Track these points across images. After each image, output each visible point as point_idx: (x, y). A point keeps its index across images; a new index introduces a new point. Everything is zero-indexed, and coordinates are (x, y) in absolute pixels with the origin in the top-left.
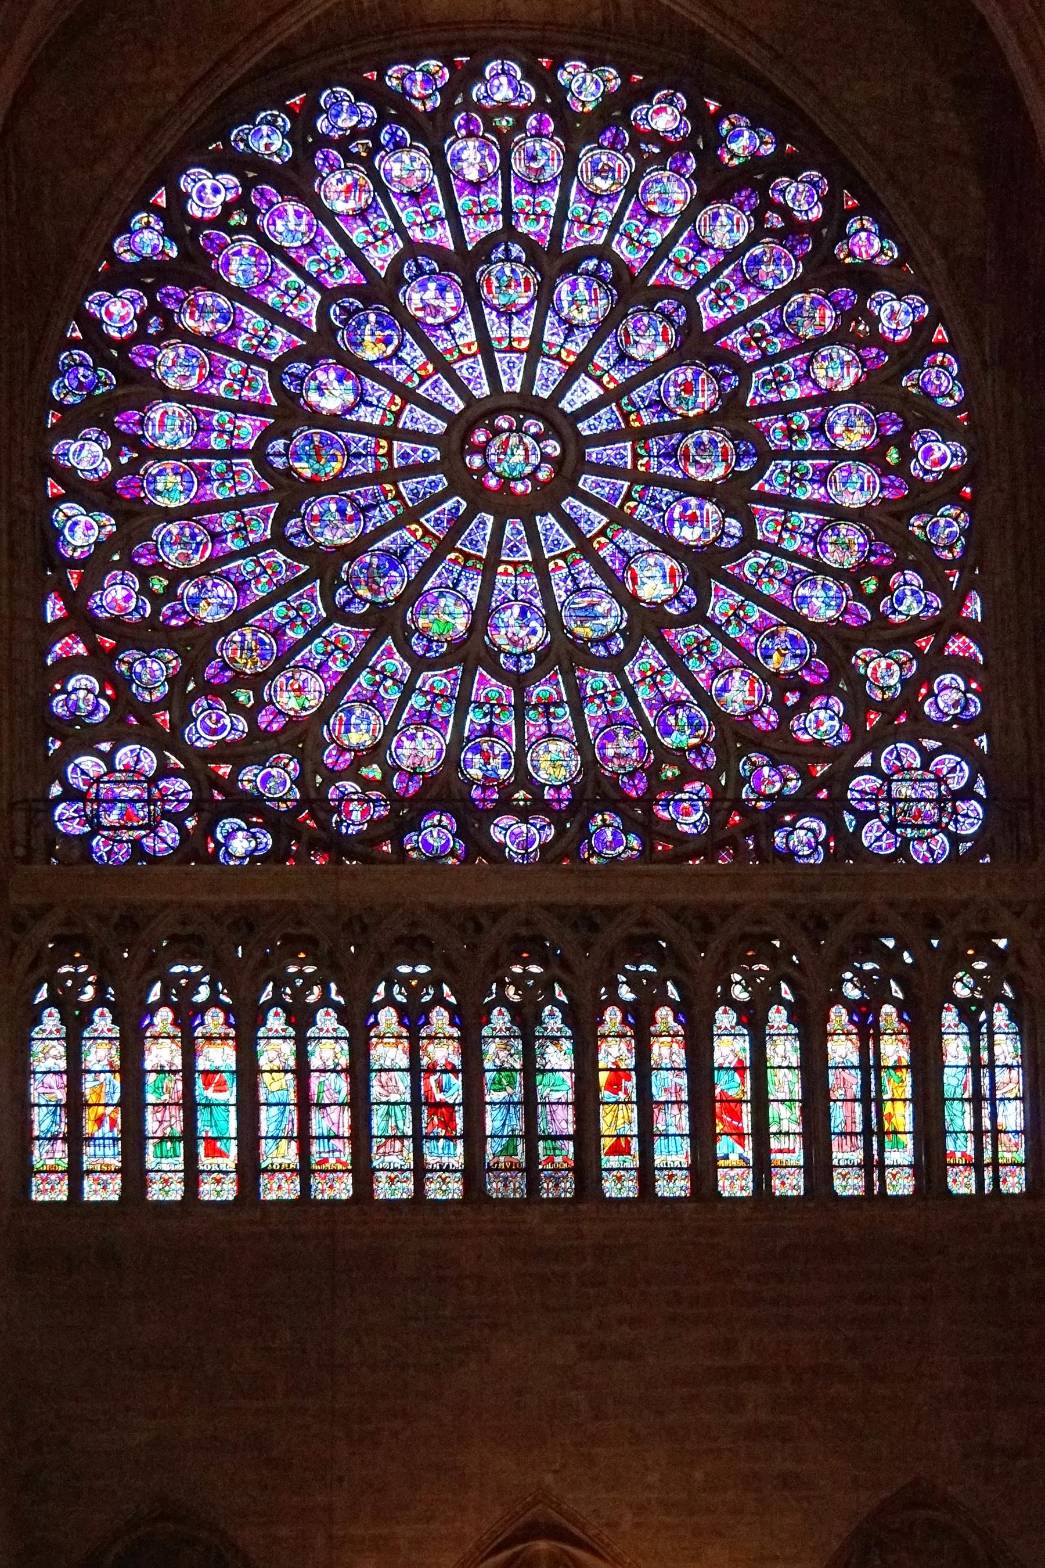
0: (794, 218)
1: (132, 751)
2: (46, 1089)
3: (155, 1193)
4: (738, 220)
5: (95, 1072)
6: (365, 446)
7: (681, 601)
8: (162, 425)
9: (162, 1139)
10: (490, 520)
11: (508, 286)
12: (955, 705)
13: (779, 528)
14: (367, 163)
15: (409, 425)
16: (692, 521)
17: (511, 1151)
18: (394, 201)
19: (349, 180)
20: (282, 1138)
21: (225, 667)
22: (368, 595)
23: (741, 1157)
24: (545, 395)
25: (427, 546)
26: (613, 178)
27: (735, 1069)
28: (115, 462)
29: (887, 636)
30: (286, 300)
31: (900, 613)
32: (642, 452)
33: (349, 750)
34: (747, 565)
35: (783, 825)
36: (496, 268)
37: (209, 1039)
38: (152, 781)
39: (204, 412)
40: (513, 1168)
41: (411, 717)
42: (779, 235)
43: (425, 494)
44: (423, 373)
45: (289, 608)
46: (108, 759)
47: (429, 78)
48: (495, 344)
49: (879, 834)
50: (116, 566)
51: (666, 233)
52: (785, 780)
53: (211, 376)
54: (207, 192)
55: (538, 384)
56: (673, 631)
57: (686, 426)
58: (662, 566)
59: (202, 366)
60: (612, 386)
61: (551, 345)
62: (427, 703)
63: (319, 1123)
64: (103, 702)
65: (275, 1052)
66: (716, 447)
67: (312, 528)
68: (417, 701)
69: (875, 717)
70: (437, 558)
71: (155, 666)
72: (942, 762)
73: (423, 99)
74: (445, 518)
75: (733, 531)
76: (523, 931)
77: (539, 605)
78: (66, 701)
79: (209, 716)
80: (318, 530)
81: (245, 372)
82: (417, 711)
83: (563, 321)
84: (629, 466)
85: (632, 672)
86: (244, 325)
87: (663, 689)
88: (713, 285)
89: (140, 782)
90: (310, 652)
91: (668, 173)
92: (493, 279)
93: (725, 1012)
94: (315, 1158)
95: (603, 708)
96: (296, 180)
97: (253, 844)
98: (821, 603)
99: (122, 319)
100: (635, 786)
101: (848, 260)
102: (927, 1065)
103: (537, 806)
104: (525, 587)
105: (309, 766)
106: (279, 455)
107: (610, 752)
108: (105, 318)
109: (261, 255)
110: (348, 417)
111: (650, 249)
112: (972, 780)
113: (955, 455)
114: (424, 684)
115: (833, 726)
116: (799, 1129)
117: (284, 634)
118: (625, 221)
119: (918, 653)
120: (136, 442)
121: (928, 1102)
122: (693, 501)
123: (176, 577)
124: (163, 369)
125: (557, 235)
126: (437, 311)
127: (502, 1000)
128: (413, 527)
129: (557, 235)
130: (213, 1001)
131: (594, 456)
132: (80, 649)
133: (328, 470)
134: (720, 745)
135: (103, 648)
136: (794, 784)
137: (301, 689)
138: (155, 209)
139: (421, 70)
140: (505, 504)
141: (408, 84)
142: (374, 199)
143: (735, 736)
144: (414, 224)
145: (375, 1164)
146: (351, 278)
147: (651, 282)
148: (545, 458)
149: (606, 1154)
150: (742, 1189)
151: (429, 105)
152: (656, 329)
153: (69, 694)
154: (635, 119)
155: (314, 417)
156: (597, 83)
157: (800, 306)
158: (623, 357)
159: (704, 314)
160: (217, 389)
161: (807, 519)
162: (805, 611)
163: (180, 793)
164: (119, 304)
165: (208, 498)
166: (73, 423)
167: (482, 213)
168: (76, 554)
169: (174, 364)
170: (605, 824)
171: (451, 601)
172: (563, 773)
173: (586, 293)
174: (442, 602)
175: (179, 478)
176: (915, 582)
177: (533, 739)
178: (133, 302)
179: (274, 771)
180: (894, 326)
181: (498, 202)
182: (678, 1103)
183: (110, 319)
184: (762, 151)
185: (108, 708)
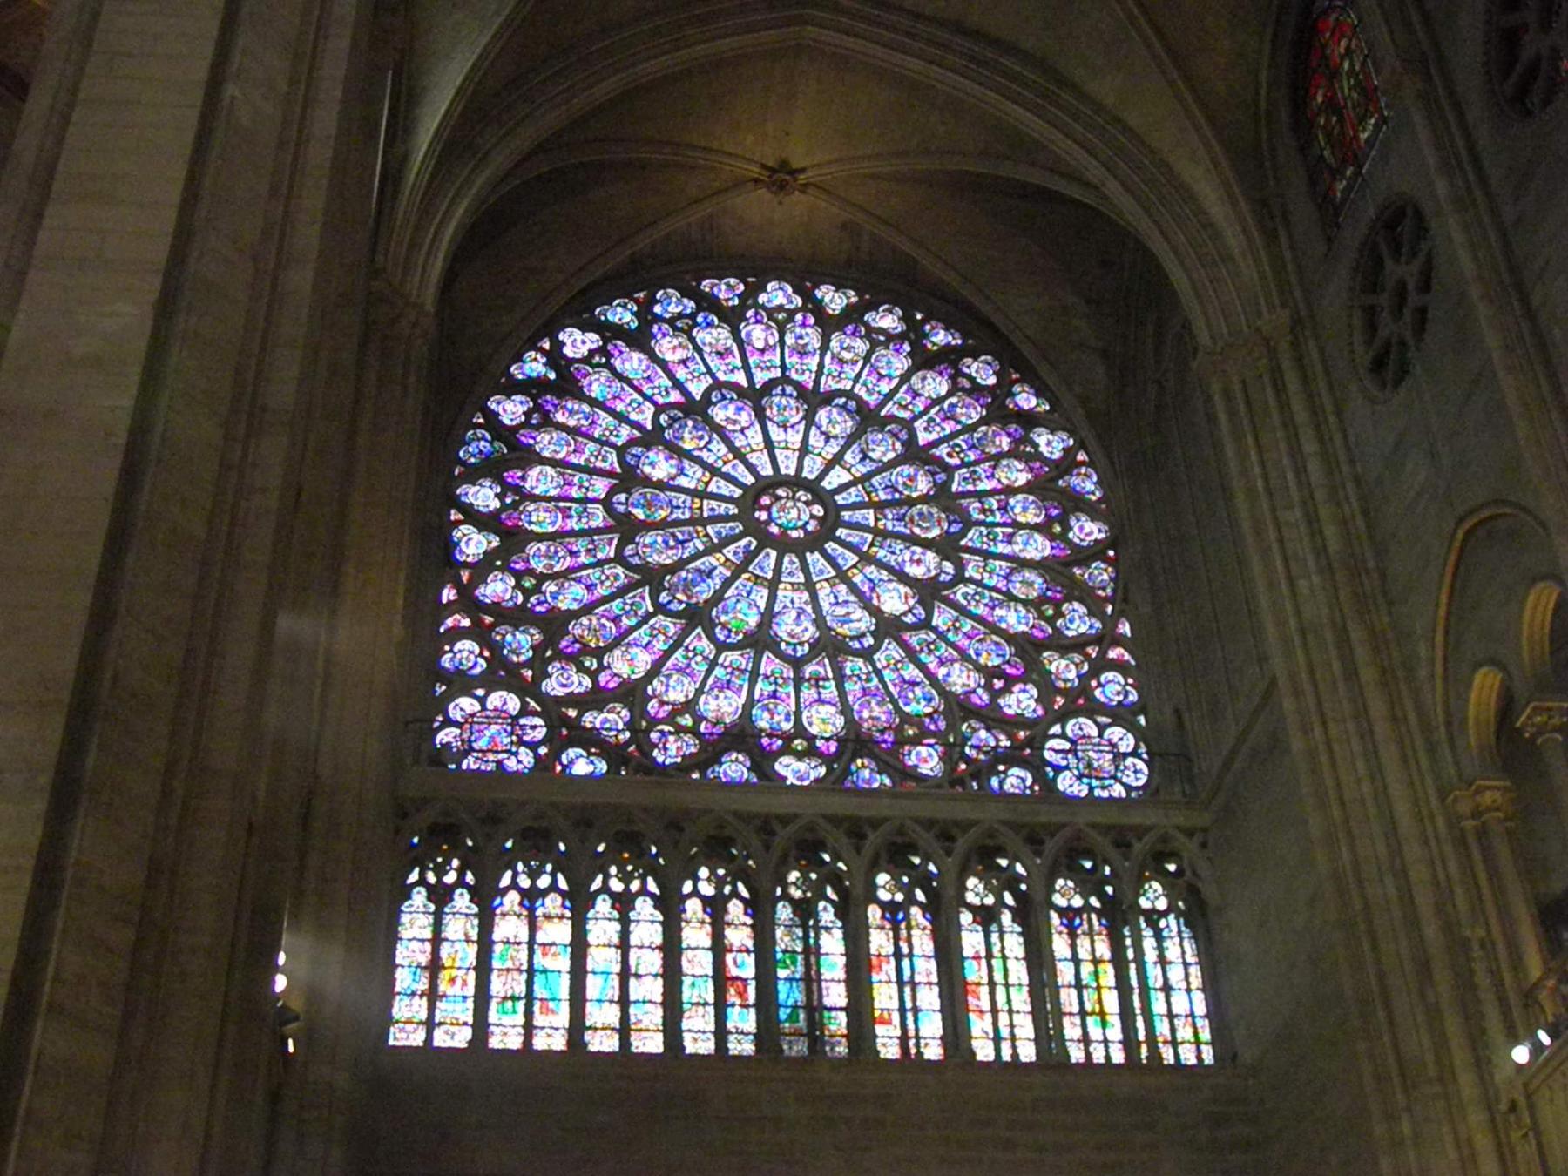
3: (495, 1043)
9: (505, 999)
10: (773, 554)
12: (1119, 693)
14: (688, 333)
16: (919, 562)
19: (675, 342)
22: (684, 598)
24: (812, 477)
25: (728, 568)
36: (776, 399)
37: (548, 917)
38: (515, 718)
40: (797, 1033)
42: (968, 392)
46: (482, 701)
47: (730, 288)
50: (498, 568)
54: (577, 343)
57: (911, 502)
63: (636, 990)
64: (481, 661)
69: (1060, 700)
70: (735, 576)
74: (741, 551)
76: (808, 836)
78: (452, 660)
94: (633, 1019)
97: (590, 768)
98: (1015, 620)
103: (811, 752)
105: (637, 711)
112: (1137, 746)
116: (1028, 1008)
119: (1087, 656)
120: (517, 489)
122: (918, 549)
123: (542, 578)
125: (817, 382)
126: (735, 422)
127: (786, 896)
129: (817, 382)
130: (553, 887)
132: (466, 623)
134: (947, 713)
135: (482, 621)
136: (1005, 743)
138: (542, 350)
140: (784, 544)
143: (959, 708)
147: (883, 413)
148: (812, 517)
155: (647, 481)
162: (1003, 626)
166: (473, 475)
170: (863, 766)
172: (830, 728)
174: (739, 606)
179: (611, 716)
182: (930, 984)
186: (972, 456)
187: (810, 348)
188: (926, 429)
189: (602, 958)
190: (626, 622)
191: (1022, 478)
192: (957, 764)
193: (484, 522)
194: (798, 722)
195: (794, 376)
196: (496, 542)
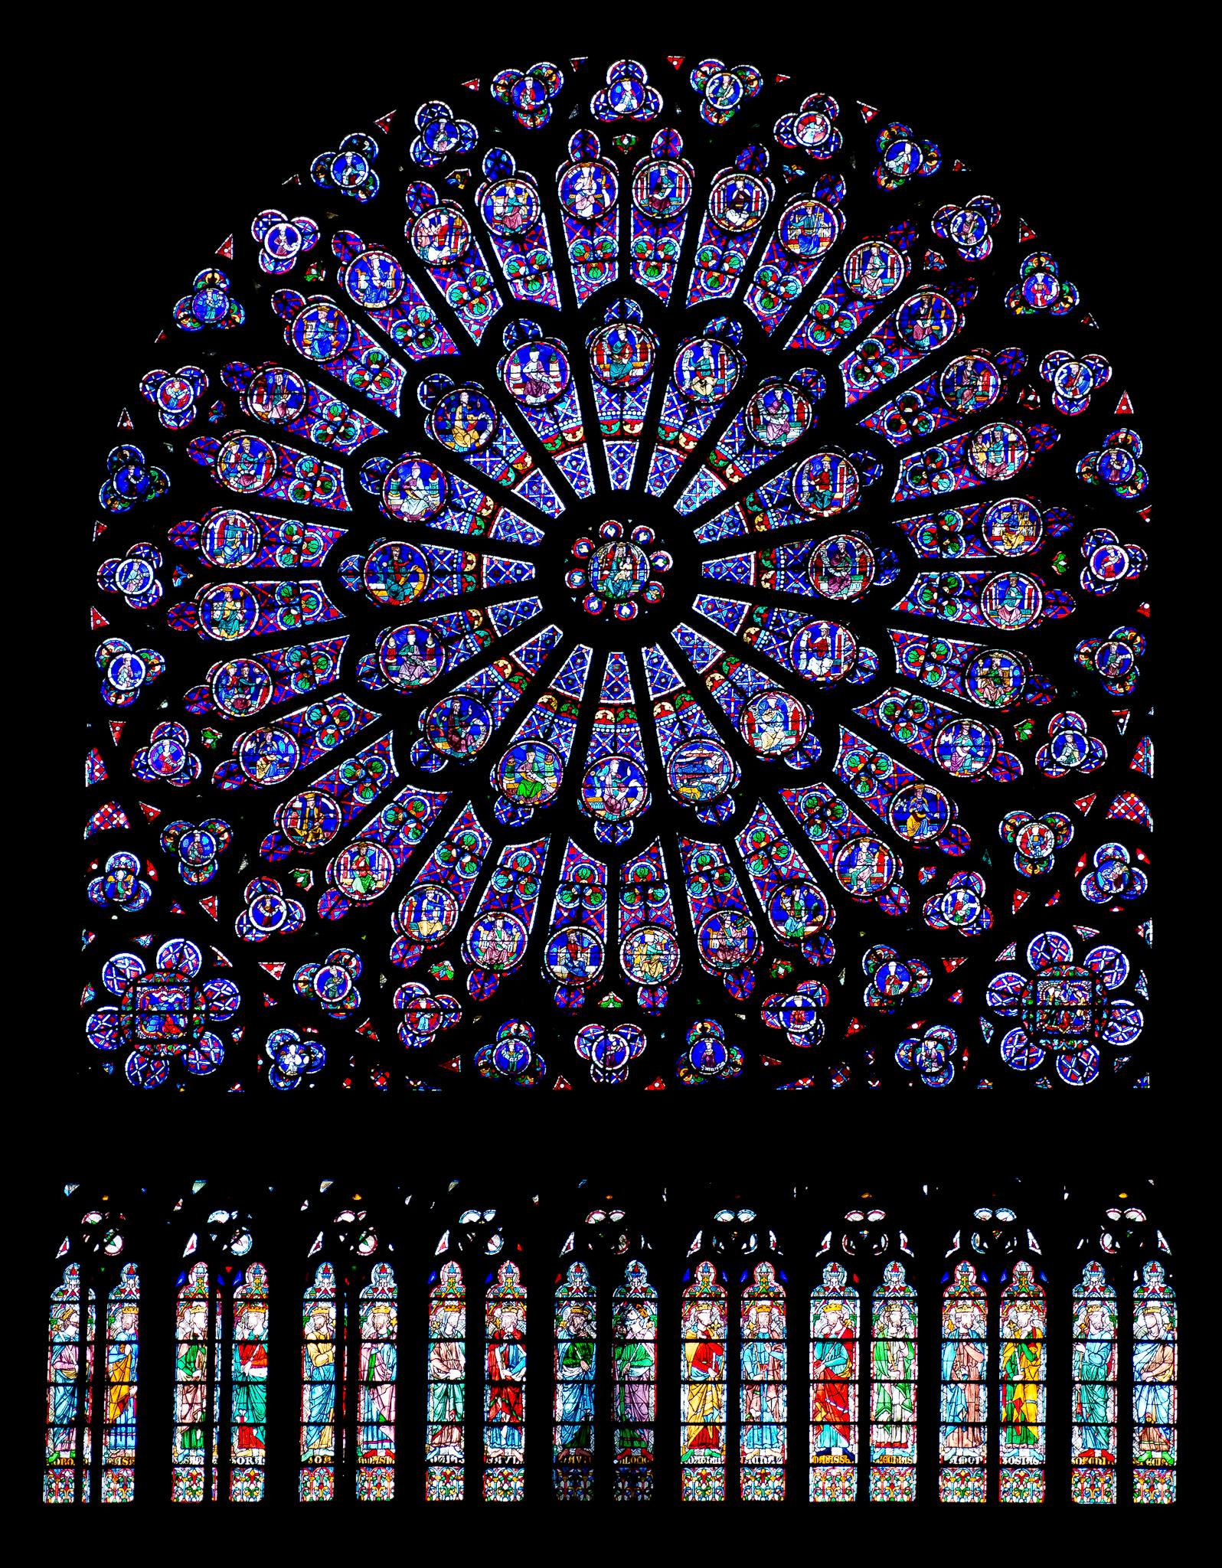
1: (175, 946)
2: (62, 1365)
5: (120, 1343)
6: (450, 562)
7: (803, 752)
8: (222, 537)
9: (192, 1426)
10: (589, 652)
11: (622, 354)
12: (1119, 880)
13: (922, 658)
16: (818, 651)
17: (583, 1440)
18: (495, 247)
19: (444, 219)
20: (325, 1424)
21: (281, 840)
23: (845, 1451)
26: (749, 210)
27: (842, 1341)
28: (167, 585)
29: (1041, 794)
30: (367, 377)
31: (1059, 765)
32: (767, 564)
35: (906, 1035)
36: (608, 331)
38: (197, 983)
42: (938, 279)
44: (520, 467)
46: (148, 955)
48: (604, 428)
53: (279, 476)
54: (283, 238)
56: (793, 791)
57: (821, 529)
58: (784, 708)
60: (736, 479)
61: (668, 429)
64: (145, 886)
65: (319, 1321)
67: (386, 665)
68: (497, 882)
71: (205, 841)
72: (1099, 955)
73: (533, 112)
75: (870, 663)
78: (104, 882)
79: (263, 901)
80: (394, 668)
81: (317, 469)
82: (498, 893)
83: (682, 398)
85: (743, 842)
86: (318, 410)
88: (859, 348)
90: (379, 821)
92: (605, 345)
93: (834, 1270)
94: (362, 1450)
96: (384, 221)
97: (306, 1060)
98: (965, 755)
99: (181, 404)
100: (741, 986)
101: (1019, 311)
102: (1059, 1340)
103: (629, 1012)
104: (627, 738)
106: (352, 573)
107: (715, 944)
109: (340, 317)
112: (1134, 977)
113: (1133, 561)
114: (506, 860)
115: (973, 910)
116: (913, 1418)
117: (352, 799)
119: (1076, 816)
121: (1059, 1384)
122: (825, 626)
123: (232, 728)
124: (224, 466)
125: (681, 283)
126: (538, 388)
128: (502, 663)
129: (681, 283)
133: (407, 592)
135: (146, 817)
137: (365, 868)
140: (608, 634)
142: (473, 242)
143: (858, 922)
145: (429, 1457)
148: (656, 573)
149: (692, 1446)
150: (844, 1492)
151: (540, 120)
153: (107, 876)
154: (778, 133)
156: (736, 87)
157: (961, 370)
158: (750, 444)
159: (846, 387)
161: (955, 646)
162: (948, 764)
164: (177, 385)
166: (122, 537)
167: (596, 260)
168: (120, 701)
169: (238, 459)
173: (712, 360)
174: (531, 756)
175: (238, 605)
176: (1078, 726)
177: (628, 928)
178: (193, 382)
180: (1070, 395)
181: (614, 244)
189: (320, 1358)
192: (846, 1024)
193: (139, 626)
196: (158, 663)
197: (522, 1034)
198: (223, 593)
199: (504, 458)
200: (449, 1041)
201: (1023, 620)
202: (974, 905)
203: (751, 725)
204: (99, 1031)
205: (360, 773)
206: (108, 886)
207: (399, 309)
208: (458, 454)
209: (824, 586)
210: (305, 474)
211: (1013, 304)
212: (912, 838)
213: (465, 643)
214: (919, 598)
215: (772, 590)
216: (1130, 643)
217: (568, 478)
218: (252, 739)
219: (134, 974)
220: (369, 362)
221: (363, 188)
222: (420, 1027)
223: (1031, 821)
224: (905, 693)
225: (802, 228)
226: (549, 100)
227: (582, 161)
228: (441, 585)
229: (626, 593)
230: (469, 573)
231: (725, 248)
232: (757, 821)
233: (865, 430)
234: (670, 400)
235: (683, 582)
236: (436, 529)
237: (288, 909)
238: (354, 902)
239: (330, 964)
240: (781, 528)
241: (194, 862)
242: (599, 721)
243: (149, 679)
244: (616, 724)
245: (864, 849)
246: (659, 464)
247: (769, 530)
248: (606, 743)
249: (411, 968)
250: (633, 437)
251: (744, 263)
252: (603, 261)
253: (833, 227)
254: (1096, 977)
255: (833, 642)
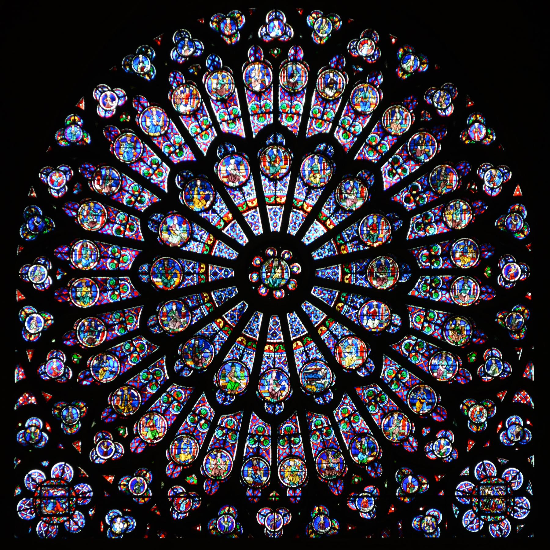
0: (438, 114)
1: (60, 466)
4: (407, 115)
6: (193, 268)
7: (366, 368)
8: (81, 254)
11: (275, 161)
12: (518, 435)
13: (422, 320)
15: (217, 254)
16: (373, 315)
18: (213, 105)
19: (187, 90)
22: (193, 366)
24: (294, 233)
25: (226, 332)
26: (336, 89)
28: (54, 278)
29: (480, 391)
30: (151, 171)
31: (489, 375)
32: (347, 270)
33: (180, 464)
34: (403, 344)
35: (417, 513)
39: (104, 245)
41: (214, 443)
43: (225, 299)
44: (226, 219)
45: (149, 373)
46: (47, 471)
47: (235, 21)
48: (267, 200)
49: (472, 519)
51: (365, 125)
52: (420, 484)
55: (290, 226)
57: (372, 253)
58: (356, 344)
59: (104, 215)
60: (331, 227)
61: (299, 201)
62: (222, 436)
64: (45, 435)
66: (389, 267)
67: (162, 321)
68: (218, 433)
72: (509, 473)
73: (230, 36)
75: (398, 322)
77: (287, 371)
79: (103, 442)
80: (166, 322)
82: (218, 439)
83: (305, 184)
84: (339, 281)
85: (337, 414)
86: (127, 188)
87: (354, 425)
88: (390, 160)
89: (63, 487)
91: (366, 85)
95: (321, 438)
96: (158, 93)
97: (126, 525)
98: (444, 369)
99: (59, 184)
100: (337, 488)
101: (467, 142)
103: (283, 503)
104: (280, 359)
106: (145, 273)
107: (324, 466)
108: (50, 184)
110: (184, 249)
111: (355, 136)
112: (525, 484)
113: (523, 271)
117: (147, 390)
118: (342, 118)
122: (375, 303)
123: (87, 353)
124: (81, 217)
131: (320, 273)
132: (33, 400)
135: (44, 398)
137: (154, 426)
139: (229, 17)
141: (222, 25)
143: (393, 456)
144: (223, 121)
146: (188, 157)
148: (293, 275)
151: (234, 40)
152: (357, 189)
153: (26, 429)
156: (328, 24)
157: (439, 172)
158: (339, 208)
159: (384, 179)
160: (112, 231)
162: (435, 374)
163: (86, 493)
164: (57, 174)
165: (105, 302)
167: (262, 113)
168: (31, 339)
169: (88, 215)
170: (320, 513)
171: (238, 368)
173: (319, 165)
176: (498, 355)
177: (282, 458)
178: (65, 172)
179: (138, 479)
180: (491, 186)
181: (270, 105)
183: (53, 184)
184: (421, 69)
185: (47, 438)
186: (426, 198)
187: (299, 88)
188: (390, 172)
190: (151, 390)
191: (465, 220)
192: (389, 508)
194: (274, 478)
195: (285, 122)
197: (231, 512)
198: (81, 283)
199: (218, 214)
200: (196, 516)
201: (470, 301)
202: (449, 447)
203: (340, 353)
204: (23, 510)
205: (150, 377)
206: (27, 435)
207: (166, 136)
208: (196, 211)
209: (375, 283)
210: (121, 221)
211: (464, 139)
212: (419, 412)
213: (201, 310)
214: (420, 289)
215: (349, 284)
216: (522, 313)
217: (250, 225)
218: (97, 359)
219: (40, 481)
220: (152, 164)
221: (148, 73)
222: (181, 509)
223: (476, 404)
224: (414, 338)
225: (362, 98)
226: (238, 30)
227: (254, 62)
228: (188, 280)
229: (279, 284)
230: (203, 274)
231: (325, 108)
232: (344, 403)
233: (395, 202)
234: (300, 186)
235: (307, 280)
236: (186, 251)
237: (115, 447)
238: (147, 443)
239: (137, 476)
240: (353, 252)
241: (69, 423)
242: (267, 351)
243: (46, 327)
244: (274, 352)
245: (396, 418)
246: (294, 218)
247: (348, 253)
248: (270, 362)
249: (176, 478)
250: (281, 205)
251: (334, 116)
252: (266, 113)
253: (377, 98)
254: (508, 484)
255: (379, 311)
